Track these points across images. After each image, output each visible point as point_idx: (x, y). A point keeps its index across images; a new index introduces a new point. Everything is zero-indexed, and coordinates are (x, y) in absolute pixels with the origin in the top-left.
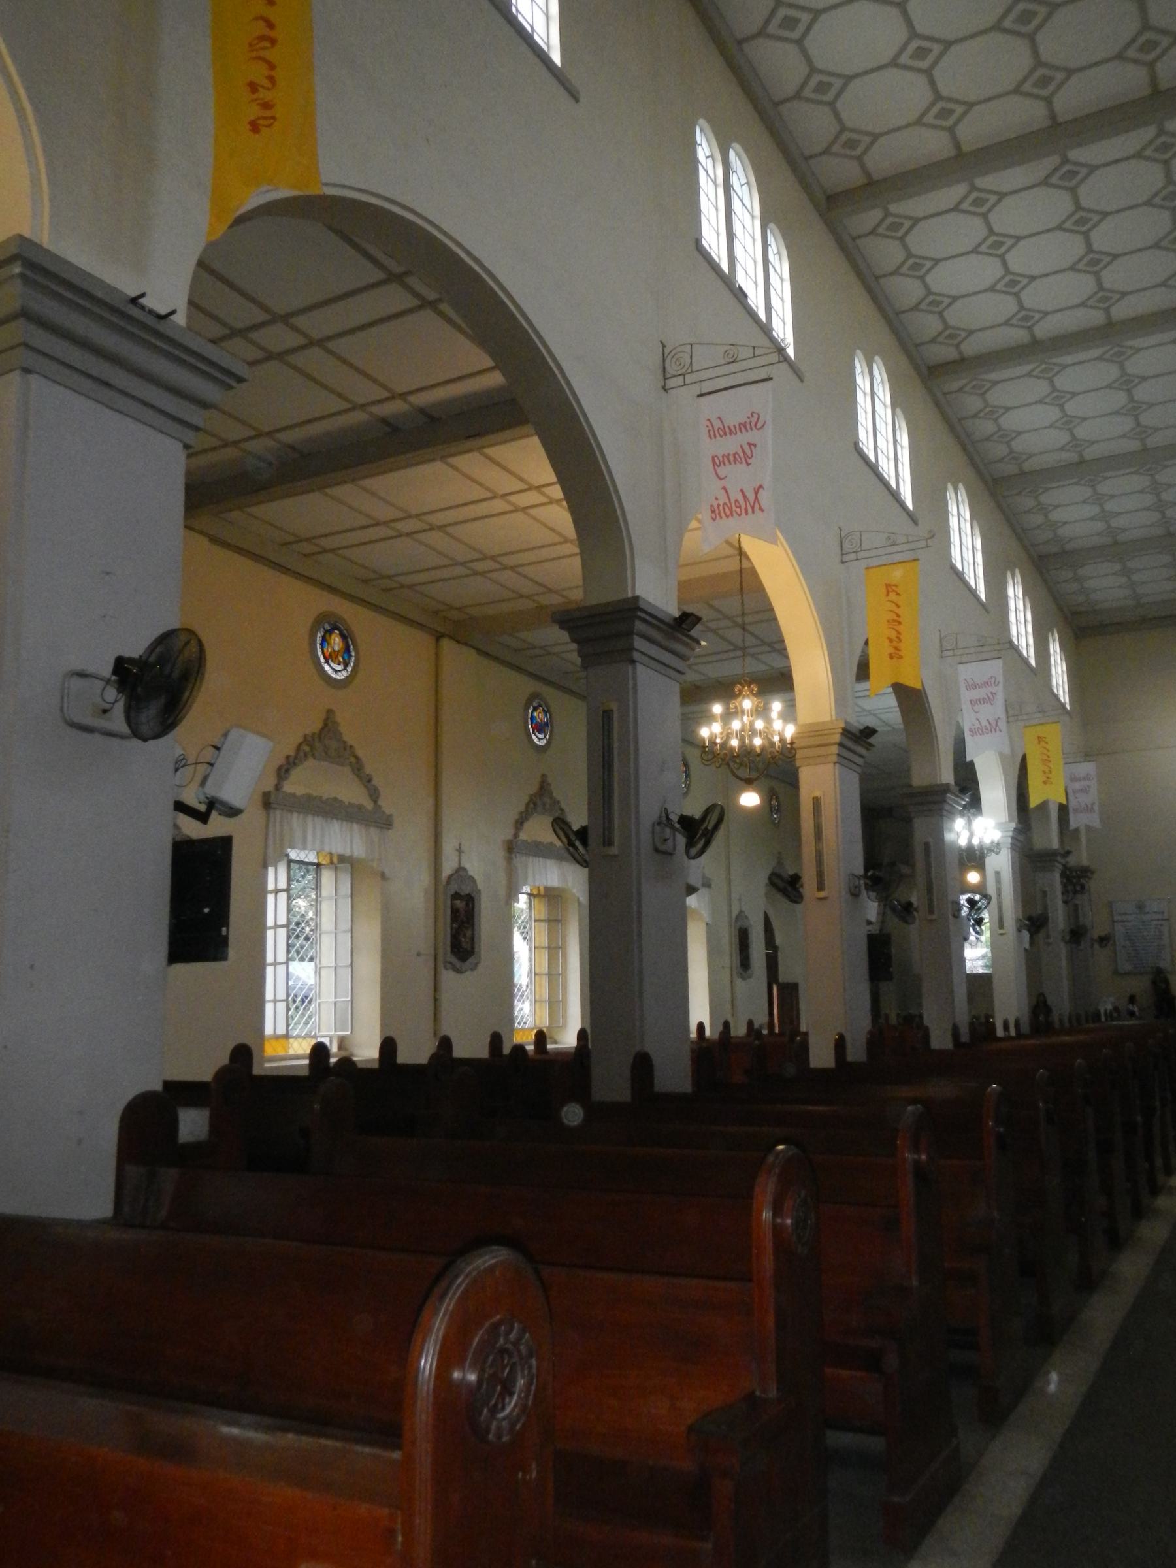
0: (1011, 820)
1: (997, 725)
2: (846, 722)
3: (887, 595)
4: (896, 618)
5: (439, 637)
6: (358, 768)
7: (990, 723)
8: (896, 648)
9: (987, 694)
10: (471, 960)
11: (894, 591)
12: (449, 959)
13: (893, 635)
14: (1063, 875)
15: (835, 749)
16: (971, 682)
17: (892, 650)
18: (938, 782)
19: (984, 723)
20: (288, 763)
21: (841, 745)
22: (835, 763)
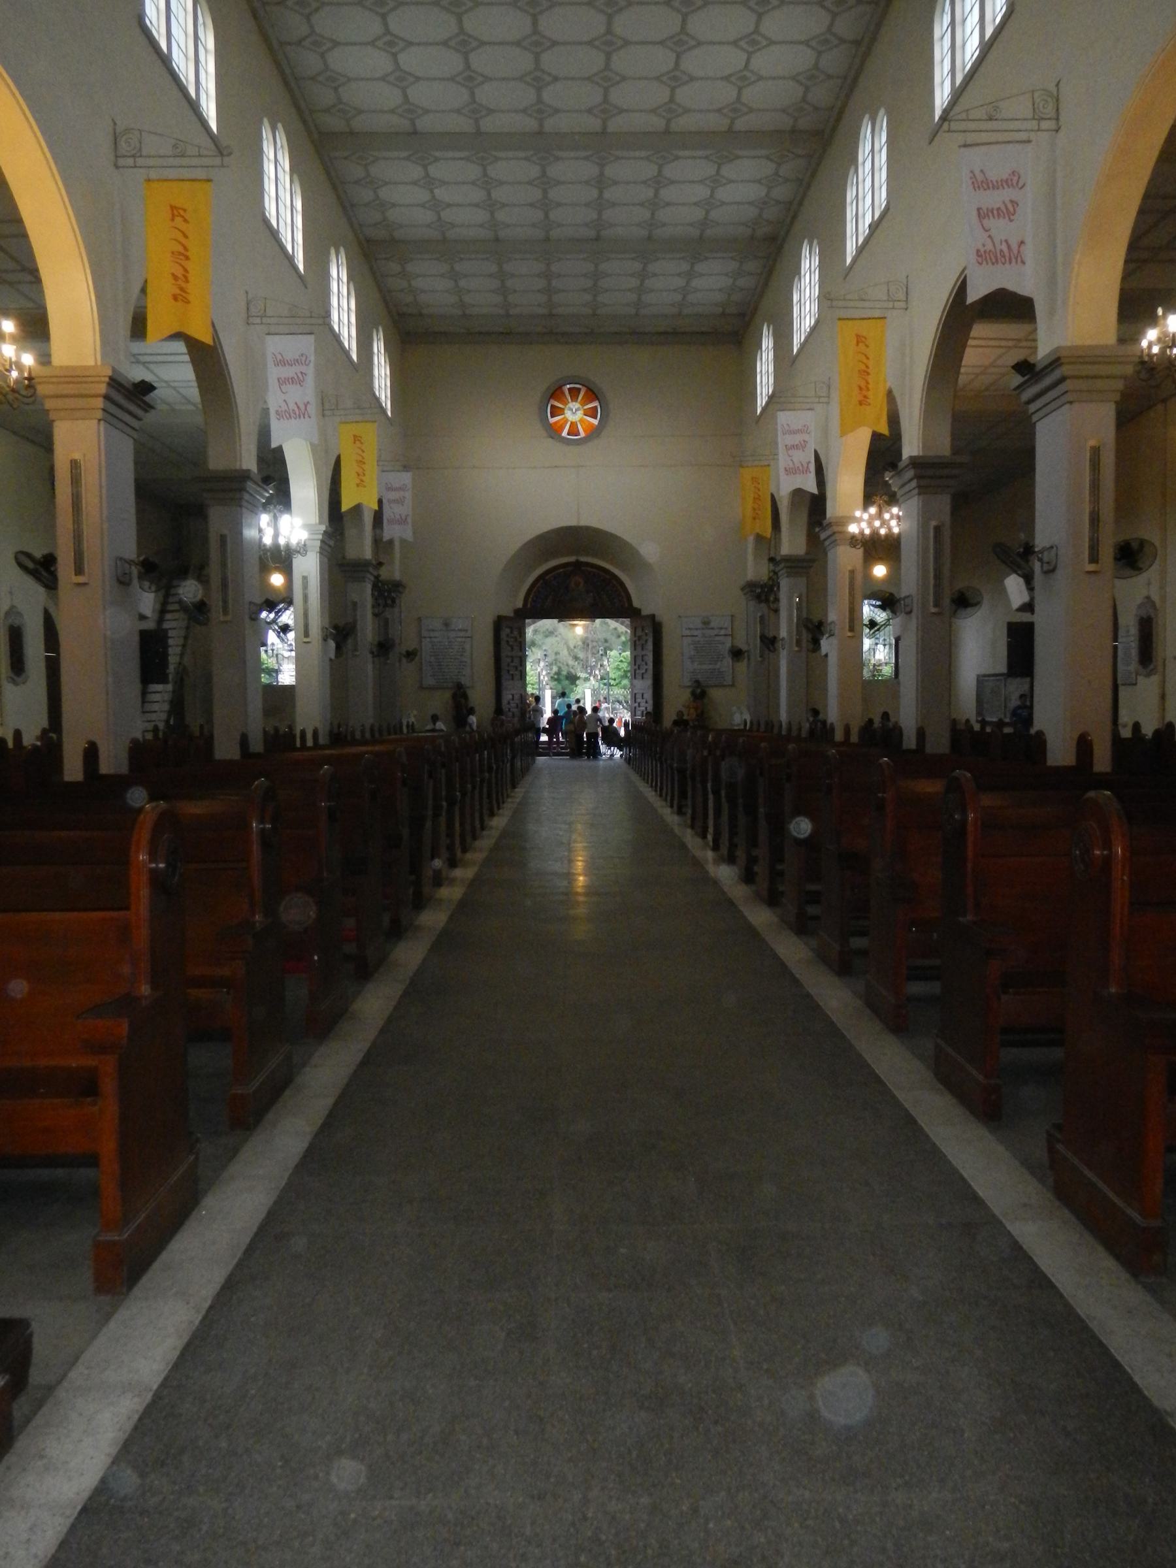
0: (320, 523)
2: (114, 370)
3: (173, 220)
4: (181, 249)
7: (298, 407)
8: (182, 289)
9: (296, 374)
13: (179, 272)
14: (375, 586)
15: (100, 403)
16: (279, 357)
18: (238, 468)
19: (292, 406)
21: (107, 397)
22: (99, 420)
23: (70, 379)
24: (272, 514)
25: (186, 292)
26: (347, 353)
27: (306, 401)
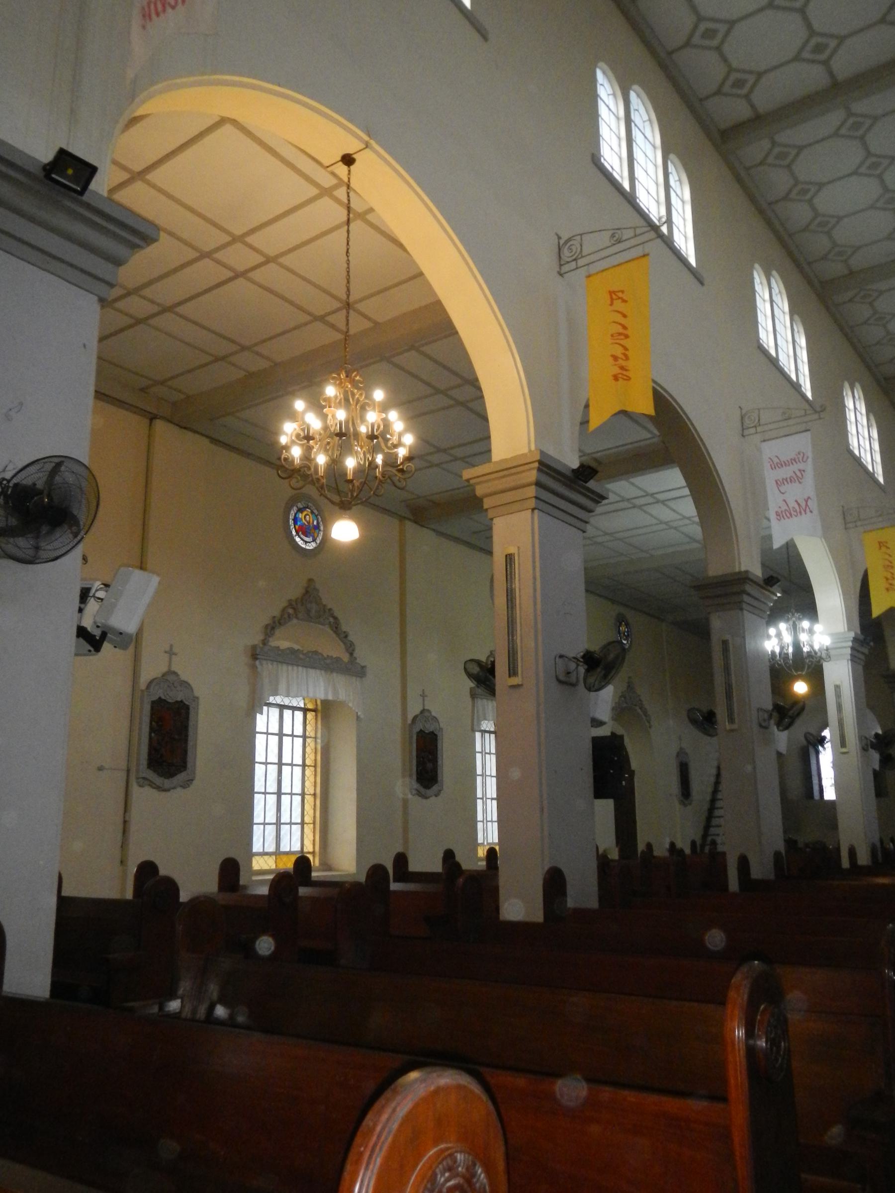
0: (849, 629)
1: (807, 505)
3: (611, 304)
4: (621, 330)
5: (152, 418)
6: (336, 627)
7: (799, 504)
10: (435, 788)
11: (619, 298)
12: (142, 775)
13: (619, 351)
15: (532, 491)
16: (776, 460)
17: (616, 370)
18: (737, 570)
19: (792, 504)
20: (274, 622)
21: (538, 484)
22: (533, 510)
23: (505, 473)
24: (791, 622)
25: (626, 370)
26: (871, 476)
27: (806, 498)
